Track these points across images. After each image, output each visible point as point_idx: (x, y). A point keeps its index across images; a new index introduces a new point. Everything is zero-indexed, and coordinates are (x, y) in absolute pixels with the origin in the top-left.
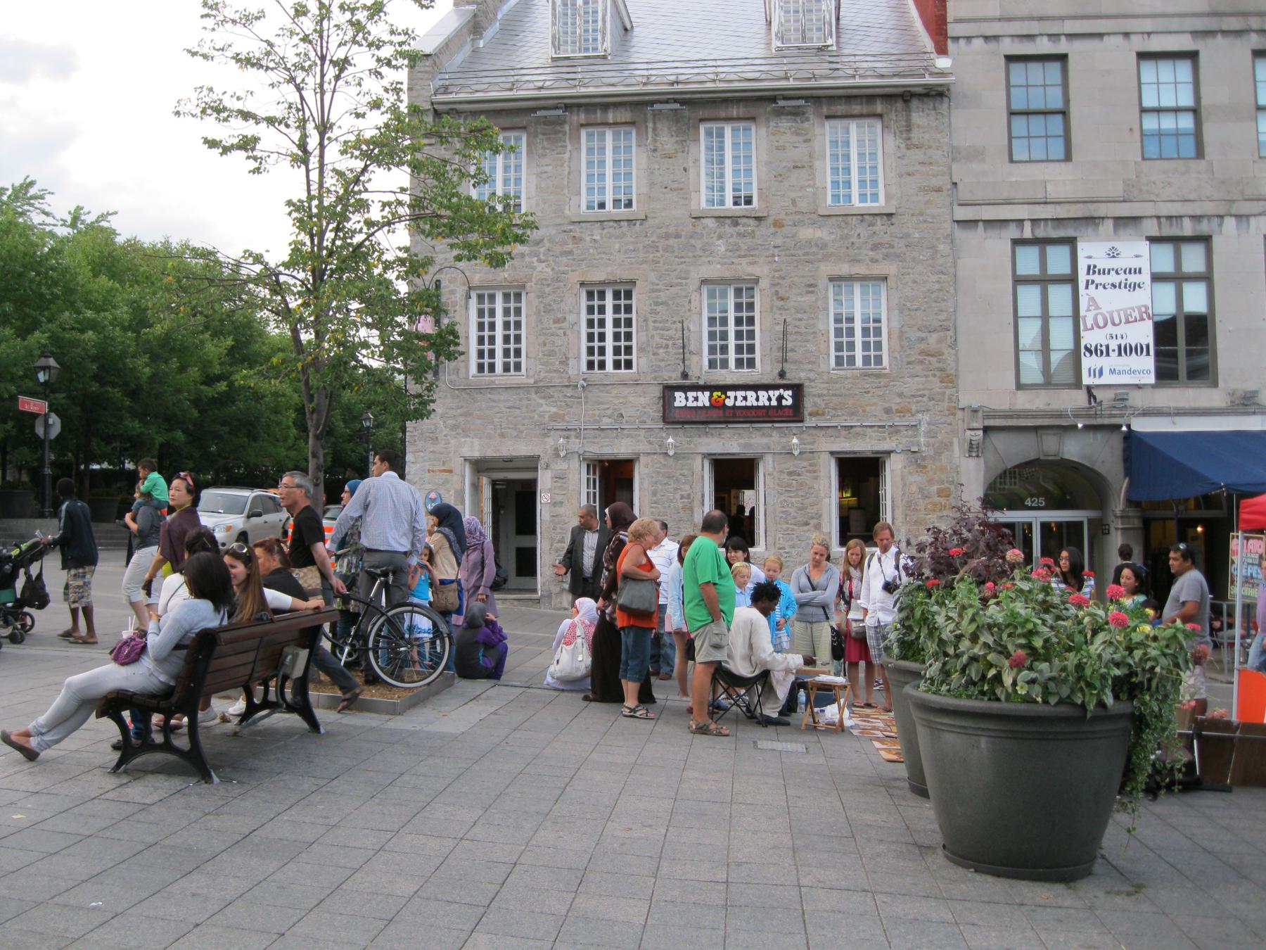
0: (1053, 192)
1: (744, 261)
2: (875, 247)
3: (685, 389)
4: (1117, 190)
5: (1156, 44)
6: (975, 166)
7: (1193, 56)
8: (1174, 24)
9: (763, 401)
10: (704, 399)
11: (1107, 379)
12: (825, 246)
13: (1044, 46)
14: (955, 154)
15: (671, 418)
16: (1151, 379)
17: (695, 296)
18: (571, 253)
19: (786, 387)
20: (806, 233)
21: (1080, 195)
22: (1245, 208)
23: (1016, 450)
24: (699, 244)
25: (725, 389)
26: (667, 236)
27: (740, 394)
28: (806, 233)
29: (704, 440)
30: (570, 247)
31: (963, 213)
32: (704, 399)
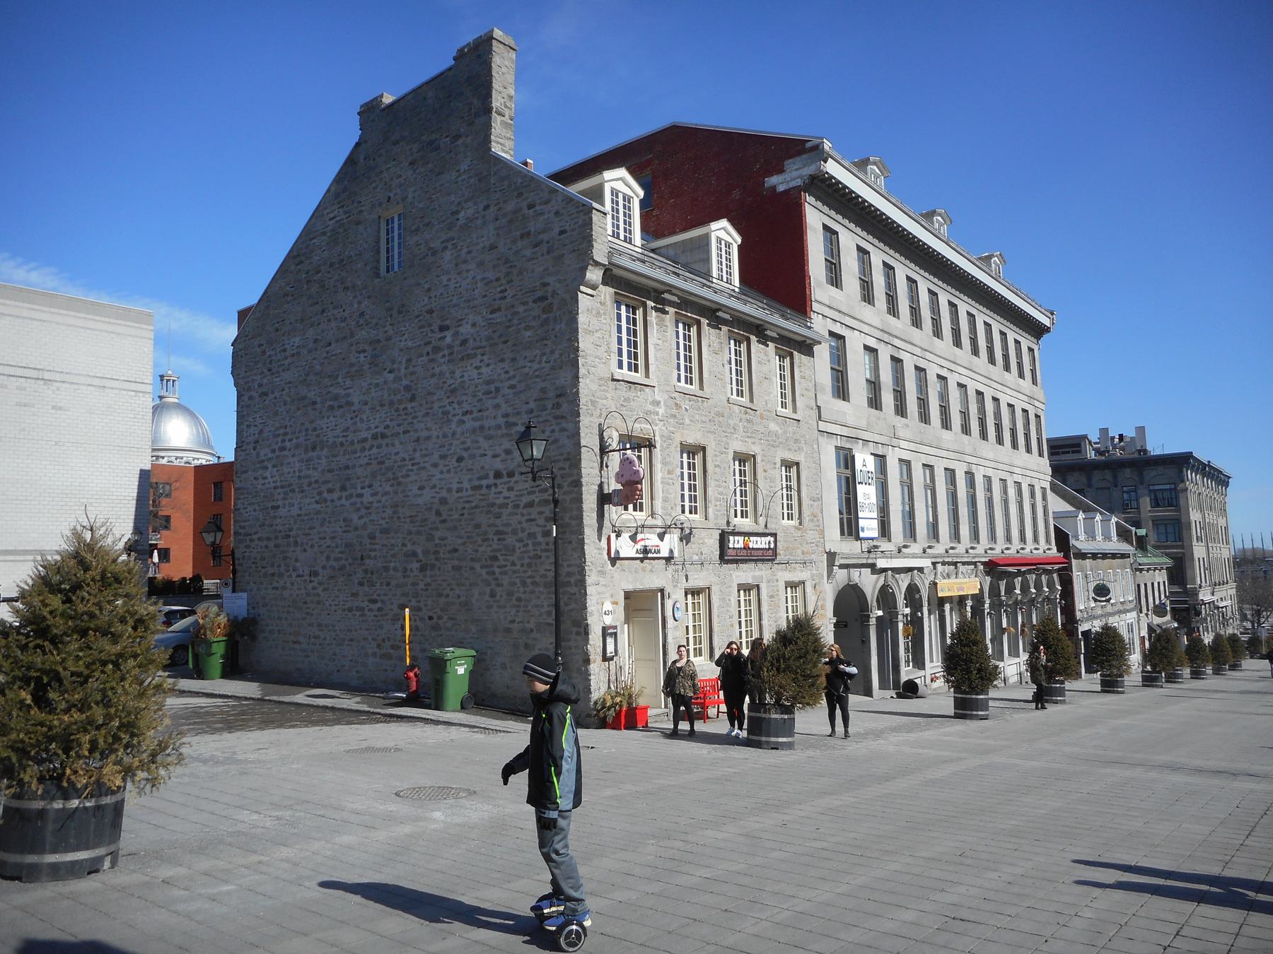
0: (850, 421)
1: (750, 440)
2: (796, 441)
4: (863, 424)
9: (763, 546)
15: (725, 556)
18: (674, 416)
20: (773, 426)
22: (895, 442)
23: (841, 576)
28: (773, 426)
29: (737, 574)
30: (674, 411)
31: (822, 426)
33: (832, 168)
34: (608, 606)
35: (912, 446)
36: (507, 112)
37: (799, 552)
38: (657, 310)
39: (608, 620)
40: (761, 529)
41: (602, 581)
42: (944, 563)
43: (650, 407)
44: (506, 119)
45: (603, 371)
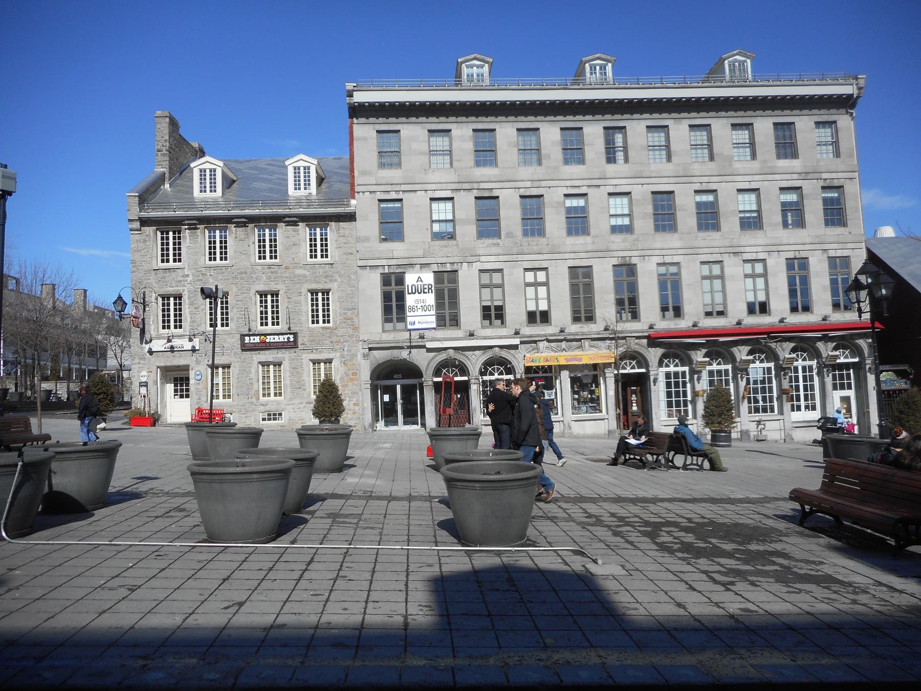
0: (396, 254)
2: (326, 277)
3: (249, 335)
5: (438, 194)
6: (366, 244)
7: (452, 199)
8: (444, 186)
10: (257, 339)
11: (417, 326)
12: (306, 276)
13: (393, 196)
14: (358, 240)
15: (245, 348)
16: (434, 325)
17: (253, 298)
19: (290, 334)
21: (407, 256)
23: (381, 356)
24: (254, 276)
25: (265, 335)
26: (241, 273)
27: (272, 337)
28: (299, 272)
29: (259, 356)
32: (257, 339)
33: (360, 97)
34: (144, 373)
35: (505, 258)
36: (164, 149)
37: (328, 342)
38: (189, 229)
39: (144, 380)
40: (285, 330)
41: (142, 362)
42: (549, 341)
43: (182, 279)
44: (164, 152)
45: (146, 267)
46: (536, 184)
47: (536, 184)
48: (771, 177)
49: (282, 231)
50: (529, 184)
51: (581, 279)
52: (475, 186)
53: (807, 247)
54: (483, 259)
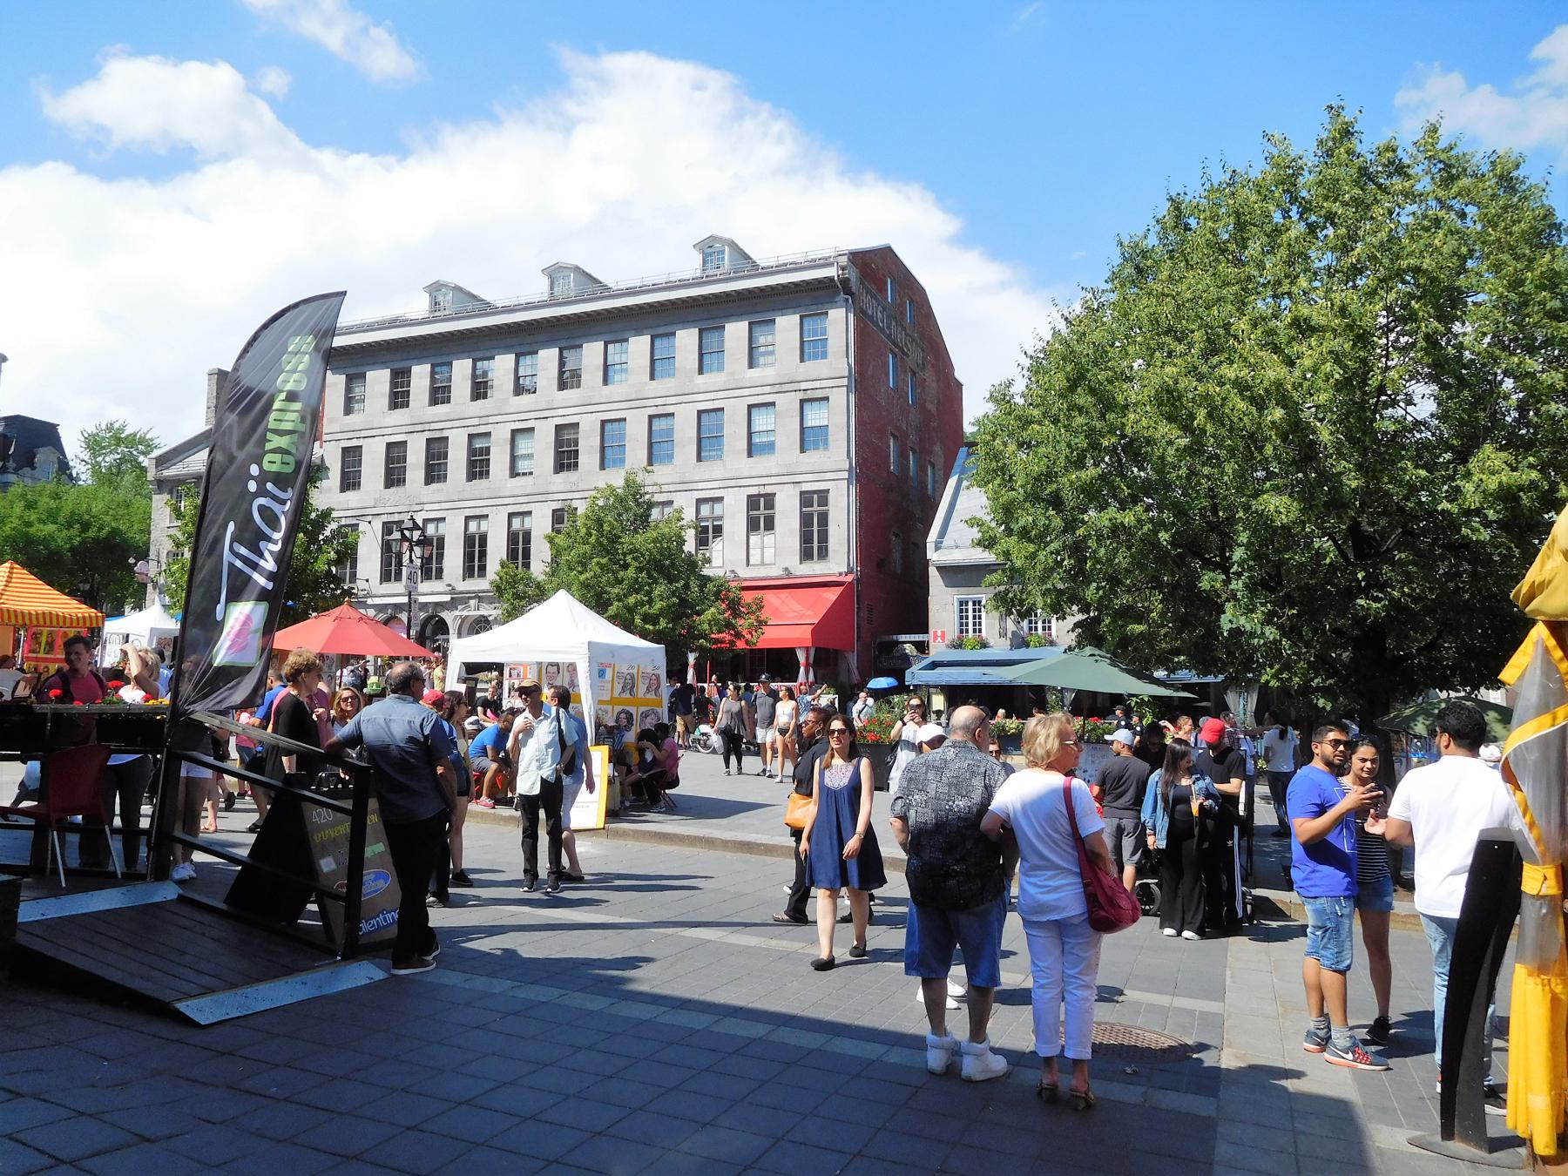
46: (484, 420)
47: (484, 420)
48: (737, 393)
49: (755, 428)
50: (476, 421)
51: (816, 507)
52: (427, 427)
53: (773, 480)
54: (427, 507)
